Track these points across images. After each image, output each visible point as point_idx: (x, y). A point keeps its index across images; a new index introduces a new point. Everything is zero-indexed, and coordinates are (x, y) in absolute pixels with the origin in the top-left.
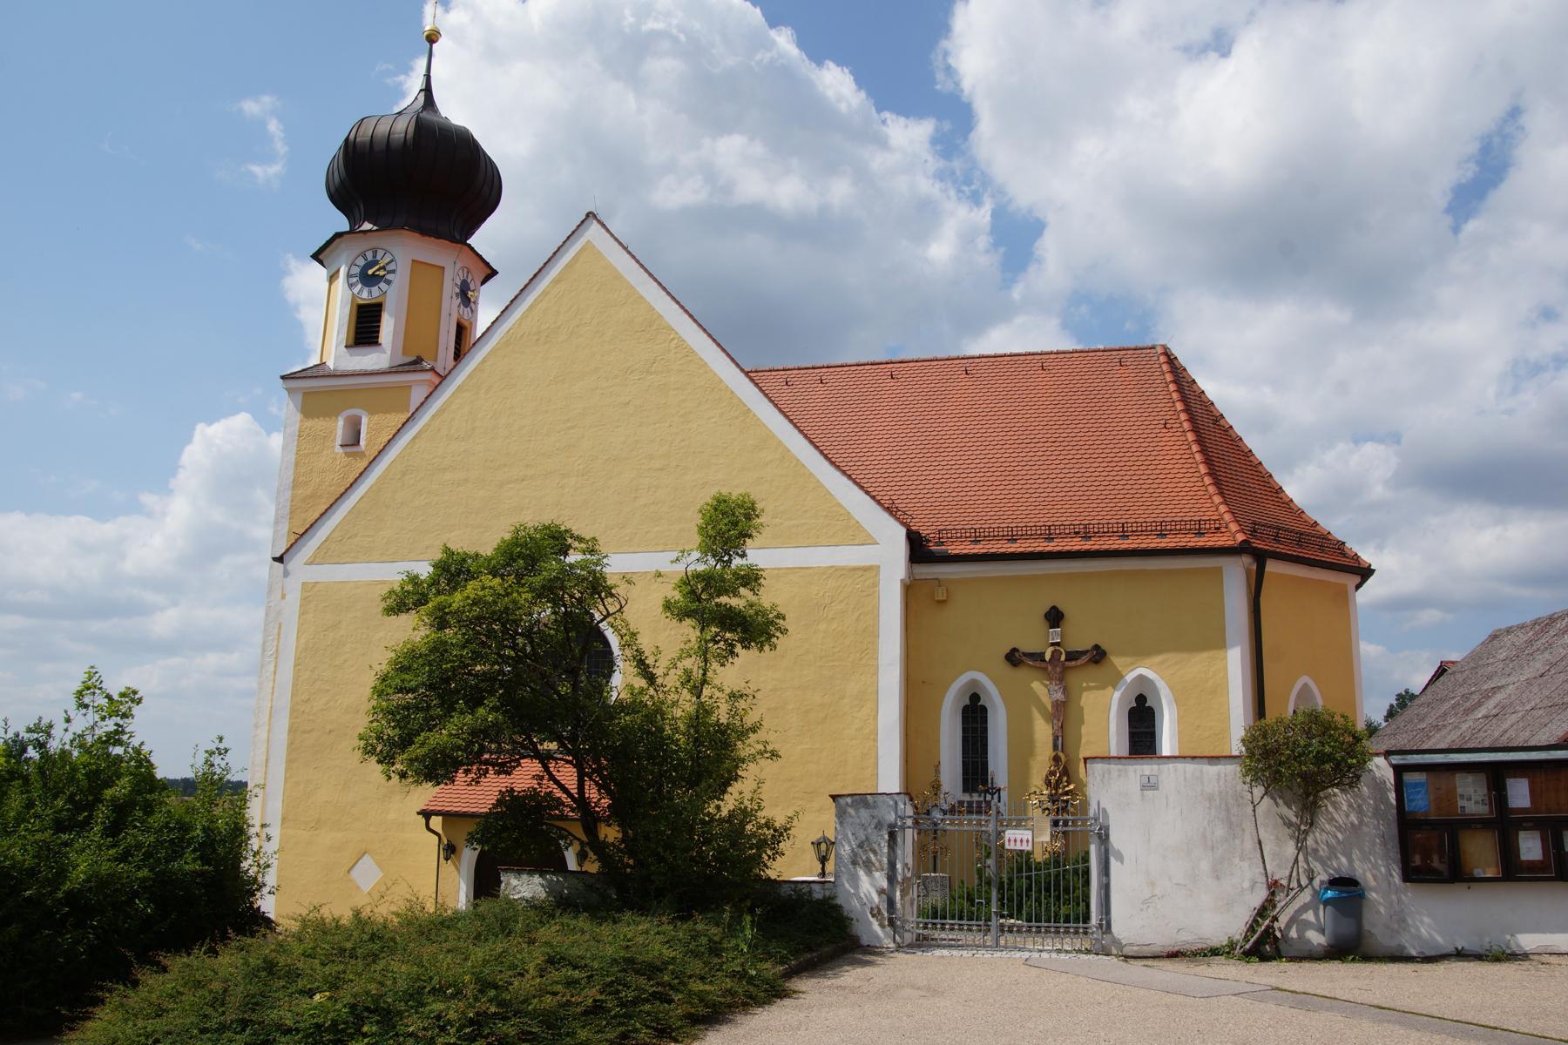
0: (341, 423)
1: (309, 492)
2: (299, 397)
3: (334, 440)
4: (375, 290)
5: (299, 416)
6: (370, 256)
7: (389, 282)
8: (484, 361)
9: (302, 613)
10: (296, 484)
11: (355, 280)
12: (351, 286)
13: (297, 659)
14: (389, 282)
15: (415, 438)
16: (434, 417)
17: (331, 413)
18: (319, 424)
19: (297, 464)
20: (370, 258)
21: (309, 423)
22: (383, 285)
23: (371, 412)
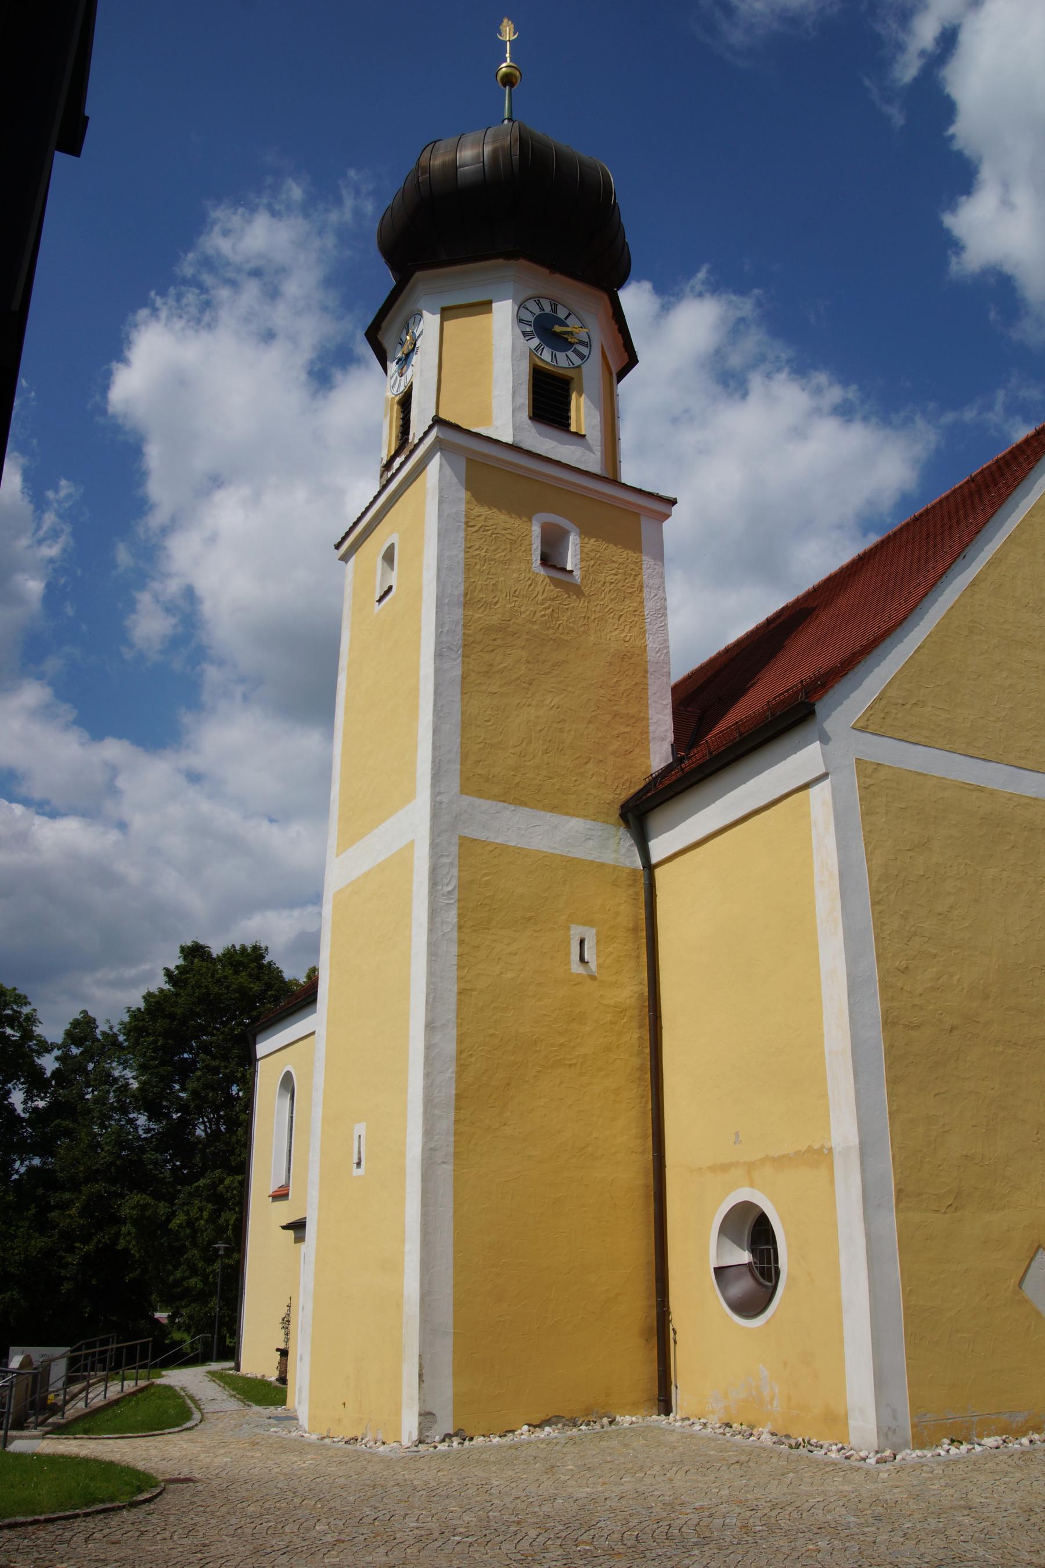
0: (536, 530)
1: (495, 620)
2: (462, 465)
3: (529, 551)
4: (561, 356)
5: (463, 494)
6: (548, 309)
7: (582, 357)
8: (1030, 514)
9: (866, 813)
10: (469, 601)
11: (528, 329)
12: (524, 334)
13: (875, 892)
14: (582, 357)
15: (973, 584)
16: (990, 564)
17: (524, 510)
18: (500, 519)
19: (468, 568)
20: (548, 309)
21: (484, 511)
22: (570, 353)
23: (586, 532)
